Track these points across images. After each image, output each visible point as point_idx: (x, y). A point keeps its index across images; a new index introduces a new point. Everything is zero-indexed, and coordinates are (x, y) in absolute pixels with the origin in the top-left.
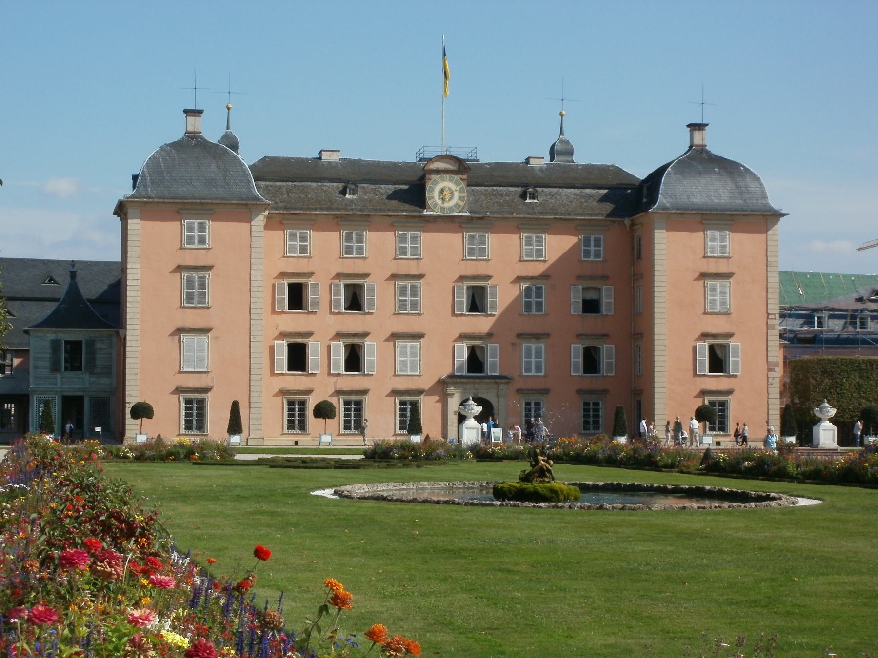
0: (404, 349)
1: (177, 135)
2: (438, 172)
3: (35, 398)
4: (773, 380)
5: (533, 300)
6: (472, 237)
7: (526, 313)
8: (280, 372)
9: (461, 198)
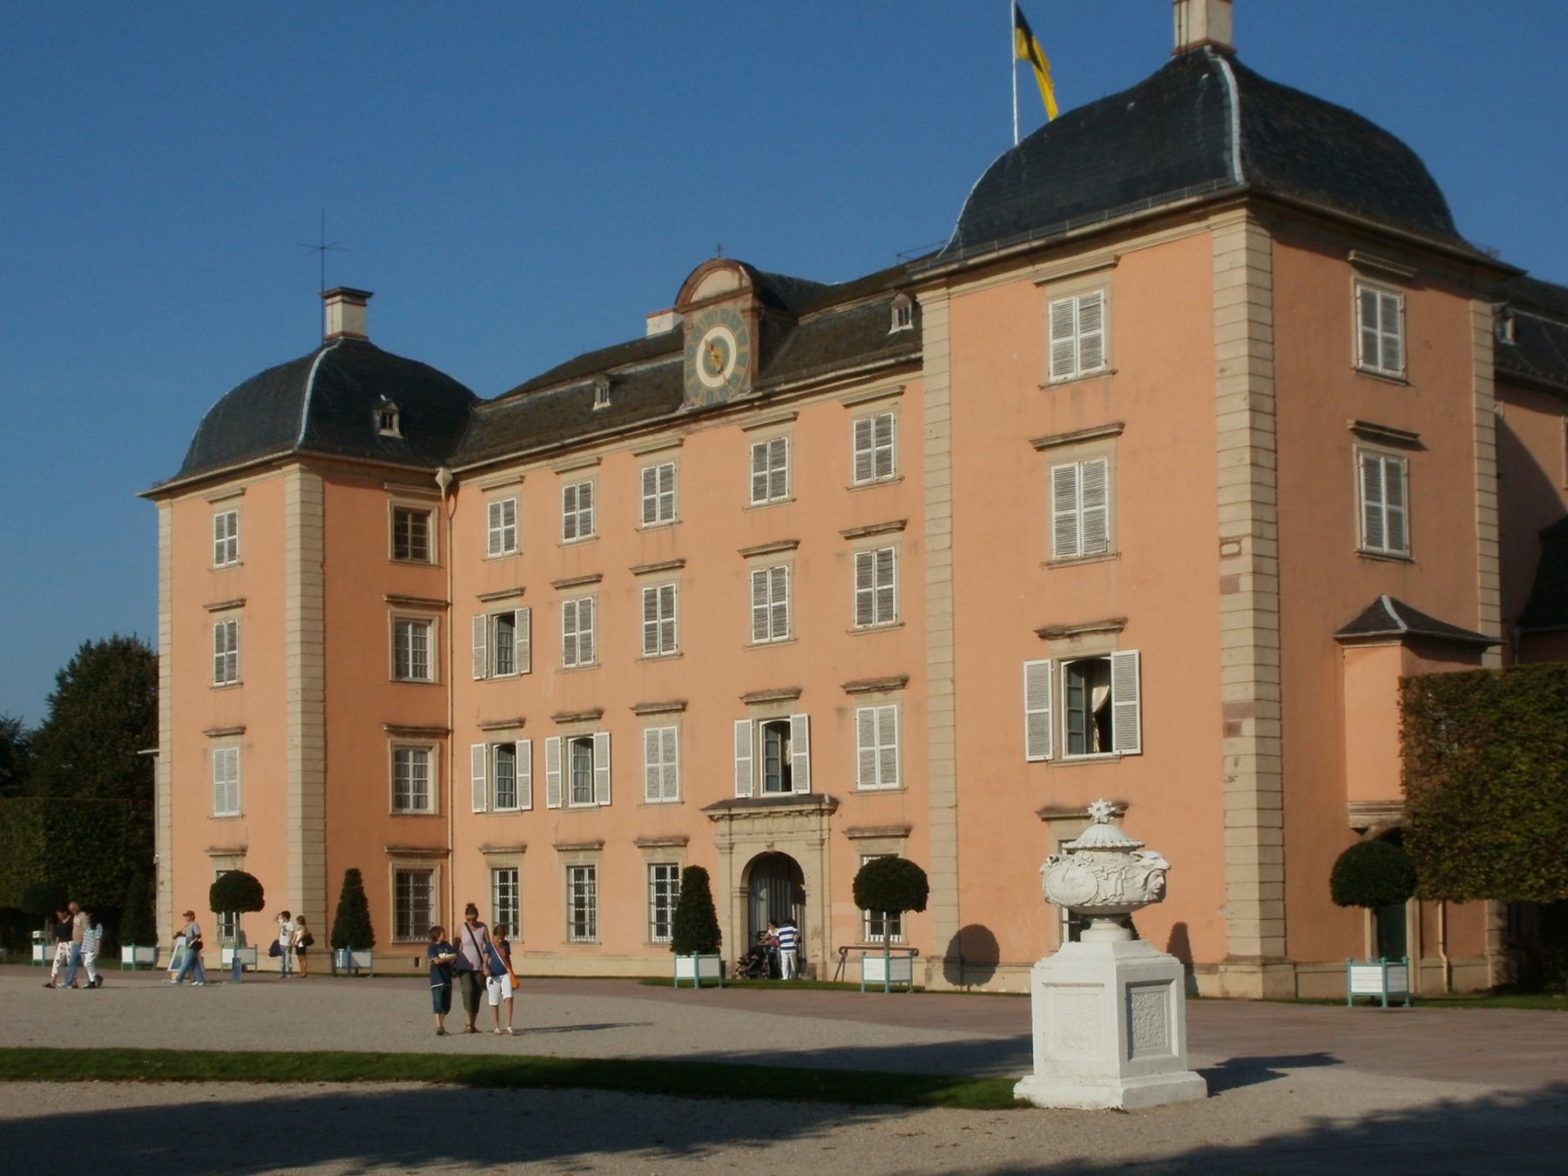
4: (1236, 764)
7: (861, 627)
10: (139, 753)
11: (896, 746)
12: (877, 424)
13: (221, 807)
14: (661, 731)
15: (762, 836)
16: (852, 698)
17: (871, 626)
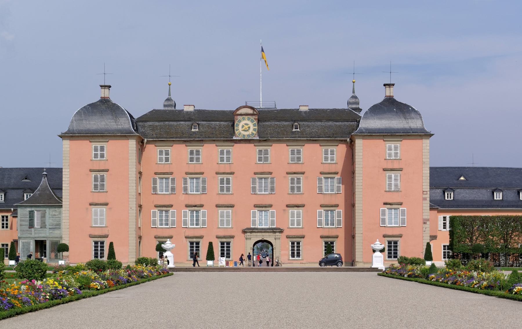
0: (222, 213)
1: (96, 99)
2: (241, 115)
3: (21, 242)
5: (296, 185)
6: (260, 151)
7: (291, 193)
8: (154, 227)
9: (254, 130)
10: (14, 205)
11: (301, 219)
12: (297, 151)
14: (225, 211)
16: (288, 208)
17: (294, 193)
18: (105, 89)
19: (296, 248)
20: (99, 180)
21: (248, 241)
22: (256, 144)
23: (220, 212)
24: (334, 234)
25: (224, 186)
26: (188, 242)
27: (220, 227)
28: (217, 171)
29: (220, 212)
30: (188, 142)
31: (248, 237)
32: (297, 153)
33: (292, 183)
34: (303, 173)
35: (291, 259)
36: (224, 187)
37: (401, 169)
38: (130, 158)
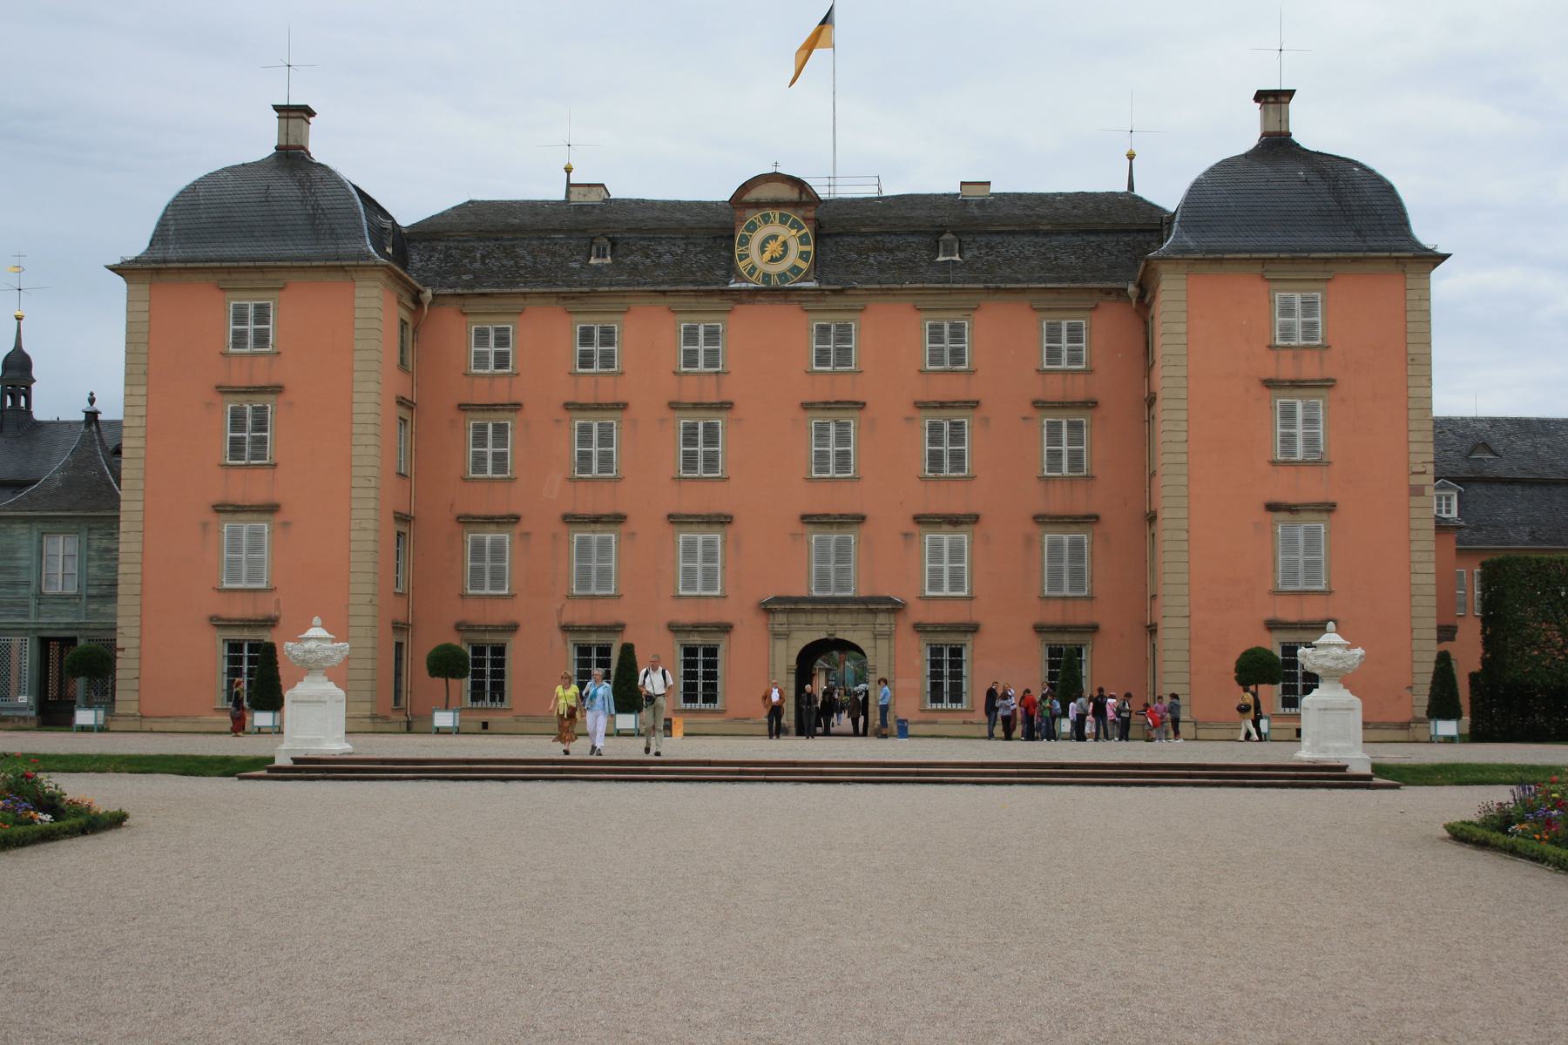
2: (758, 205)
6: (823, 330)
7: (931, 474)
9: (803, 256)
12: (950, 328)
13: (237, 579)
14: (700, 538)
15: (824, 626)
16: (916, 529)
17: (942, 474)
18: (290, 121)
19: (946, 670)
20: (249, 422)
21: (781, 645)
22: (809, 306)
23: (681, 540)
24: (1081, 616)
25: (697, 451)
26: (570, 646)
27: (681, 593)
28: (674, 398)
29: (681, 540)
30: (573, 298)
31: (779, 629)
32: (952, 335)
33: (933, 441)
34: (974, 405)
35: (929, 707)
36: (695, 453)
37: (1327, 380)
38: (358, 345)
